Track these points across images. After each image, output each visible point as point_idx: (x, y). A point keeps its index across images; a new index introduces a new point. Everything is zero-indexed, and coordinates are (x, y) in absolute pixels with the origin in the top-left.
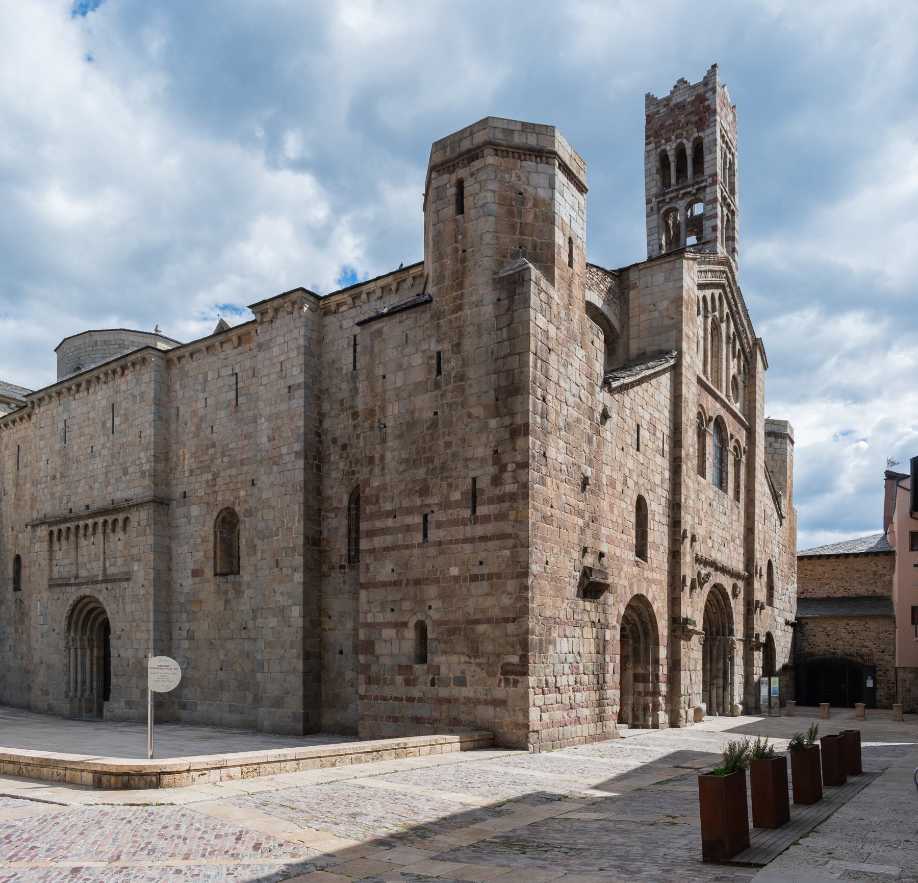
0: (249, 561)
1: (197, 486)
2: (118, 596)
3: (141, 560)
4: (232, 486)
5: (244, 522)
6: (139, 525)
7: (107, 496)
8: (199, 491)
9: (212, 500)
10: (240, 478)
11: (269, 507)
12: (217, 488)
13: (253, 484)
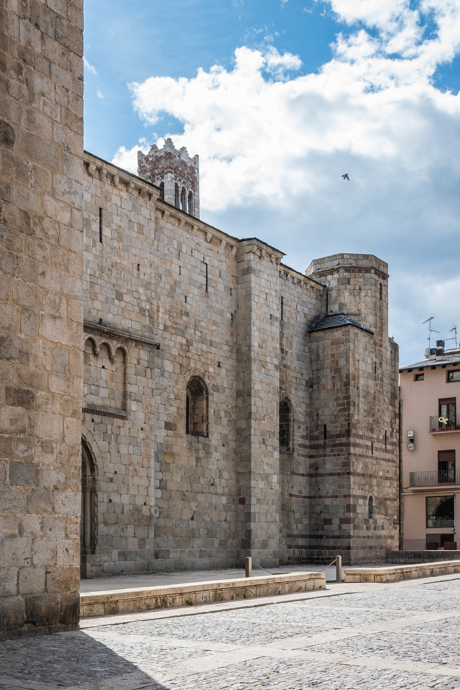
0: (216, 428)
1: (172, 344)
2: (109, 432)
3: (141, 402)
4: (204, 360)
5: (213, 395)
6: (139, 363)
7: (94, 312)
8: (174, 349)
9: (185, 364)
10: (210, 356)
11: (259, 397)
12: (190, 355)
13: (219, 366)
